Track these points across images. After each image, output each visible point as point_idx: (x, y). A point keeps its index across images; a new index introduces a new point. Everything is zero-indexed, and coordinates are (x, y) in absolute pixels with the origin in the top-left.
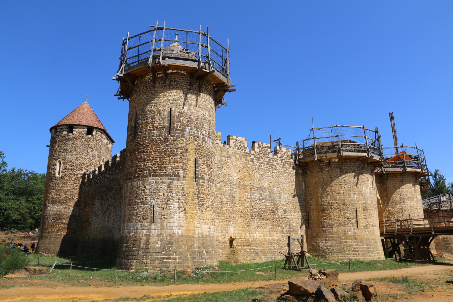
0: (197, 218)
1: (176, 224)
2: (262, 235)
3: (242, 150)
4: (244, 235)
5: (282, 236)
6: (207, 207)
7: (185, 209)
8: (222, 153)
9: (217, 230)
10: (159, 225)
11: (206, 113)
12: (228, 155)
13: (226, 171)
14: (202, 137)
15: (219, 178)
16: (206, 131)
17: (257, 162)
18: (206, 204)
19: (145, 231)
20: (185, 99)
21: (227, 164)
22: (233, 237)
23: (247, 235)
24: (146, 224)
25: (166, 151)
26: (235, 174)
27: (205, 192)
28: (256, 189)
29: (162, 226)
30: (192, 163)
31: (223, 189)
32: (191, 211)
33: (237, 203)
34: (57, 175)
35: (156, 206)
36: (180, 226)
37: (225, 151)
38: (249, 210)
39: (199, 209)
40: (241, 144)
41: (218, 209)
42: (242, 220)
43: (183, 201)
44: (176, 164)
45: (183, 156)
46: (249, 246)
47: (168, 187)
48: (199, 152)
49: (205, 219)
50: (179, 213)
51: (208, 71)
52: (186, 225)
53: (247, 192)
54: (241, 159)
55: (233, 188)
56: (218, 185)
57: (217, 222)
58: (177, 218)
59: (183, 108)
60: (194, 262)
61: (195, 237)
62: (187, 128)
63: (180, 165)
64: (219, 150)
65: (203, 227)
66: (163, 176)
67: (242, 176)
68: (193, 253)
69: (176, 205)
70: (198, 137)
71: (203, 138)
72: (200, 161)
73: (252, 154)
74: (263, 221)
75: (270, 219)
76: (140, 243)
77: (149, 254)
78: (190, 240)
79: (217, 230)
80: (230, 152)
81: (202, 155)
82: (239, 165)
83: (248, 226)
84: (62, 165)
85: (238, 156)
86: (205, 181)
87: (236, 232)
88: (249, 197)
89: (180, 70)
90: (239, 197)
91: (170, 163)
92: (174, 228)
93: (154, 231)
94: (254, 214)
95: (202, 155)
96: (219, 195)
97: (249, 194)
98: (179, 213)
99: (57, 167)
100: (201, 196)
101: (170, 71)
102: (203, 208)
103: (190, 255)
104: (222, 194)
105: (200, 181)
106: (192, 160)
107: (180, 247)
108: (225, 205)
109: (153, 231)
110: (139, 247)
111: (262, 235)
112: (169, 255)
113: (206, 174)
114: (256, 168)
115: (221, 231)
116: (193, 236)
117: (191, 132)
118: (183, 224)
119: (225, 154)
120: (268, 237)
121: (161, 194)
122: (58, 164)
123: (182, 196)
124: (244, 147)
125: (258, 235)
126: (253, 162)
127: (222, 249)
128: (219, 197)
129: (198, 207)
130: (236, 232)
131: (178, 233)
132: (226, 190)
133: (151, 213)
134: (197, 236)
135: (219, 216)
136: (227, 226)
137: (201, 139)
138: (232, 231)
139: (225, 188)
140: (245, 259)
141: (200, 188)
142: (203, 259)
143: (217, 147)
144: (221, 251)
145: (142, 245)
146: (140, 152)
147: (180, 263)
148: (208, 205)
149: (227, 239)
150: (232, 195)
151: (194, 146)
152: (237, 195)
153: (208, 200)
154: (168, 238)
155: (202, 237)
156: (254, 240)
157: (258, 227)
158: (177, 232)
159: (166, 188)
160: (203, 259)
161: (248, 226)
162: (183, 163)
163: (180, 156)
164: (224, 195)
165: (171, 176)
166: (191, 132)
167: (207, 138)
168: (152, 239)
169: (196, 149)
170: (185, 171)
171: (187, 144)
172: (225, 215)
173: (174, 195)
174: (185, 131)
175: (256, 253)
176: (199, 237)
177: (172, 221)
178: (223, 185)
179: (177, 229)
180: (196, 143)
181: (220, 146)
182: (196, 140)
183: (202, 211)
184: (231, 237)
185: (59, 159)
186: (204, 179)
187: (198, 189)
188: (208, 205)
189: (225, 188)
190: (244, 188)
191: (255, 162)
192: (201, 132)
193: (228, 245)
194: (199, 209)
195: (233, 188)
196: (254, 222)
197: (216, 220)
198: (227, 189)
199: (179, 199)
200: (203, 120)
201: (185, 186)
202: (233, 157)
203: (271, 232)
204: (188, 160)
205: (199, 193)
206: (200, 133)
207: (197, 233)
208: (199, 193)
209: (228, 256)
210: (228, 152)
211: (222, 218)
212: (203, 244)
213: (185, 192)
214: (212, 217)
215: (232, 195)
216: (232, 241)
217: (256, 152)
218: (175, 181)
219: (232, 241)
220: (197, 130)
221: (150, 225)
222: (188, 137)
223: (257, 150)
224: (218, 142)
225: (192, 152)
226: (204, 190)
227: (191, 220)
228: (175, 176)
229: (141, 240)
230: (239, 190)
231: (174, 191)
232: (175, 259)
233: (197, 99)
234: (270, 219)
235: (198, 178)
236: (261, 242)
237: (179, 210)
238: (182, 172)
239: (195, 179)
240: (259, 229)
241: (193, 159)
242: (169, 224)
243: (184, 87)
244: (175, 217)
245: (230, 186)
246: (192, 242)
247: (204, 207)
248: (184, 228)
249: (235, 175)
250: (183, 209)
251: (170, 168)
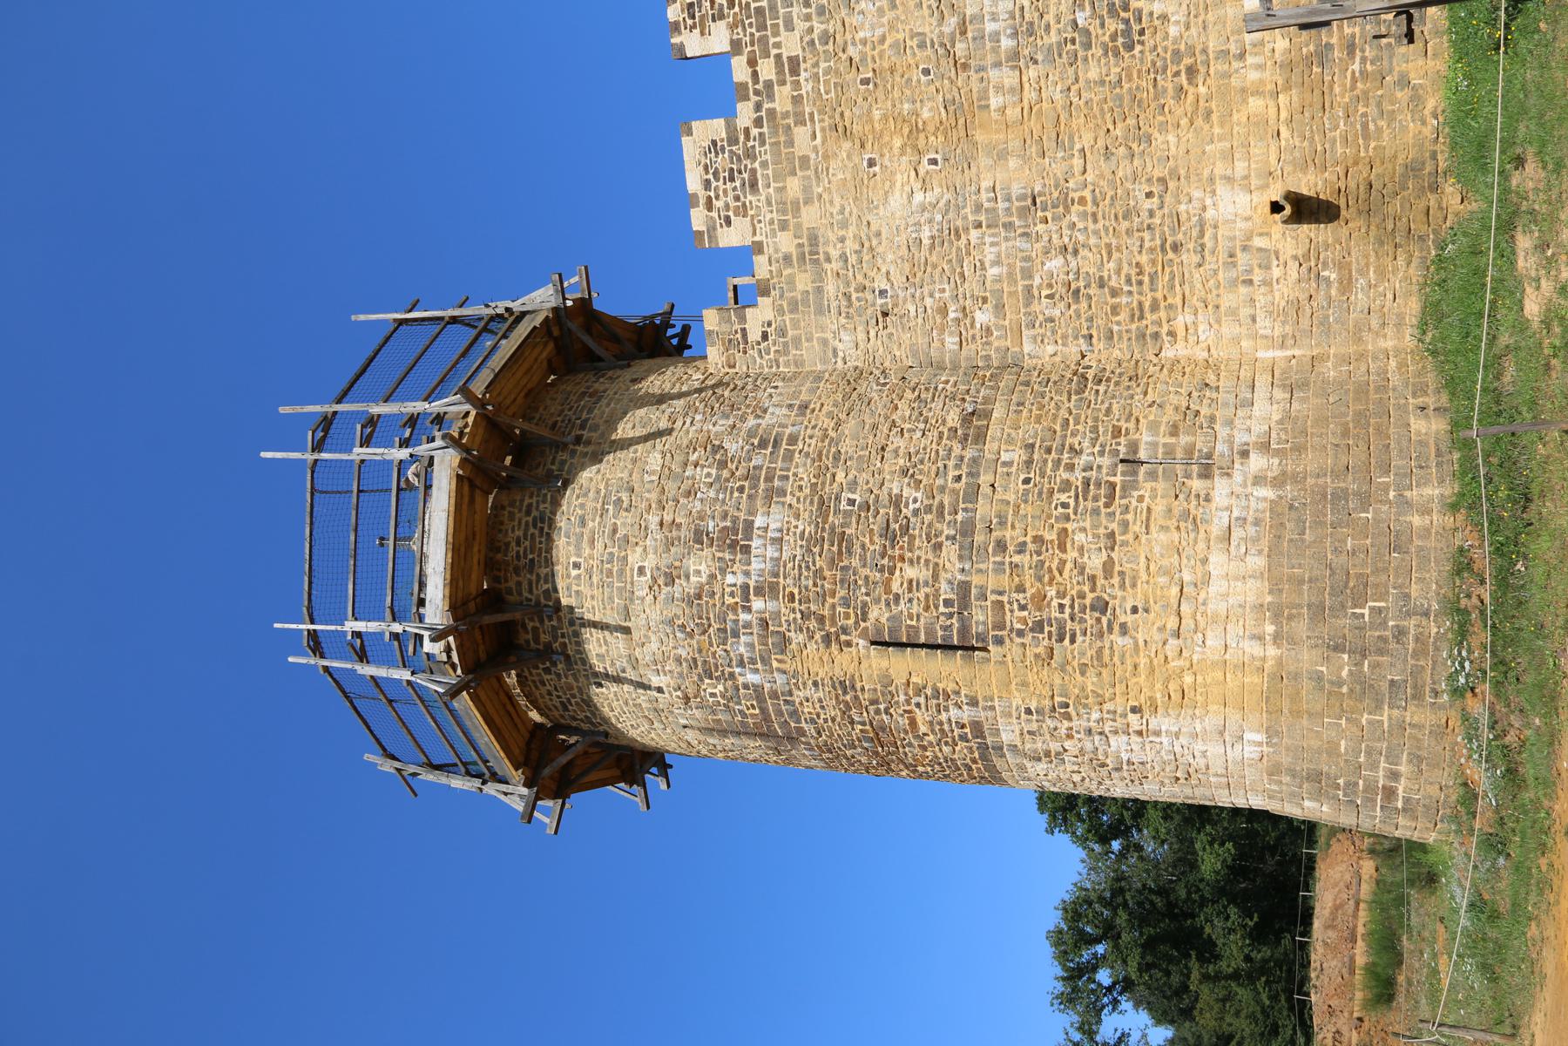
1: (1215, 750)
3: (750, 154)
4: (1255, 104)
6: (1108, 567)
7: (1134, 710)
8: (806, 302)
11: (641, 570)
12: (802, 257)
13: (889, 269)
14: (757, 604)
15: (944, 311)
16: (723, 571)
17: (790, 26)
18: (1093, 579)
20: (618, 680)
21: (853, 259)
23: (1253, 76)
26: (897, 200)
27: (1028, 578)
28: (952, 22)
30: (900, 664)
31: (998, 280)
33: (1058, 169)
36: (1221, 733)
37: (791, 281)
38: (1093, 74)
39: (1124, 629)
40: (722, 161)
41: (1115, 310)
42: (1163, 128)
43: (1095, 716)
44: (923, 729)
45: (874, 702)
48: (833, 623)
49: (1175, 590)
50: (1158, 733)
51: (451, 639)
52: (1213, 708)
53: (984, 95)
54: (805, 160)
55: (978, 208)
56: (982, 317)
57: (1189, 319)
58: (1183, 740)
59: (660, 690)
60: (1418, 696)
61: (1280, 662)
62: (741, 680)
63: (921, 717)
64: (796, 325)
65: (1222, 608)
67: (897, 142)
68: (1364, 689)
71: (759, 591)
72: (878, 614)
73: (755, 75)
78: (1295, 698)
79: (1233, 312)
80: (786, 242)
81: (846, 602)
82: (839, 171)
83: (1192, 72)
85: (794, 186)
86: (976, 580)
87: (1240, 167)
88: (1008, 77)
89: (510, 698)
90: (1025, 159)
92: (1234, 754)
94: (1113, 25)
95: (846, 602)
96: (1035, 307)
97: (993, 74)
98: (1158, 733)
100: (1055, 614)
101: (534, 715)
102: (1122, 600)
103: (1378, 708)
104: (1029, 289)
105: (980, 617)
106: (885, 664)
107: (1332, 750)
108: (1088, 262)
112: (1370, 788)
113: (935, 577)
114: (826, 37)
115: (1243, 290)
116: (1272, 677)
117: (753, 661)
118: (1212, 721)
119: (804, 282)
123: (1068, 717)
124: (733, 140)
126: (795, 64)
127: (1346, 285)
128: (1042, 307)
129: (1120, 641)
130: (1240, 167)
131: (1260, 744)
132: (997, 263)
134: (1272, 651)
135: (1155, 307)
136: (1207, 239)
137: (772, 605)
138: (1237, 207)
139: (993, 271)
140: (1416, 100)
141: (1014, 618)
142: (1400, 633)
143: (782, 332)
144: (1360, 298)
147: (1416, 759)
148: (1095, 563)
150: (1024, 213)
151: (812, 647)
152: (1016, 176)
153: (1072, 554)
155: (1277, 617)
160: (1400, 633)
161: (1192, 72)
162: (908, 702)
163: (878, 712)
164: (1028, 274)
166: (753, 661)
167: (756, 565)
169: (827, 640)
171: (815, 684)
172: (1144, 259)
174: (758, 689)
176: (1277, 638)
177: (1201, 762)
178: (972, 286)
179: (1238, 747)
180: (797, 638)
181: (769, 314)
182: (784, 641)
183: (1135, 610)
184: (1276, 208)
187: (1020, 633)
188: (1095, 563)
189: (993, 271)
190: (962, 116)
191: (791, 44)
192: (734, 608)
194: (1124, 629)
195: (978, 208)
196: (1164, 18)
198: (993, 252)
200: (677, 590)
202: (810, 216)
205: (1039, 627)
206: (744, 617)
207: (1254, 649)
208: (1039, 627)
209: (1393, 238)
210: (787, 258)
212: (1318, 611)
213: (1047, 703)
215: (1024, 213)
217: (736, 47)
220: (736, 635)
222: (780, 679)
223: (718, 39)
224: (754, 335)
225: (843, 663)
226: (1021, 589)
227: (1188, 679)
230: (984, 161)
232: (1395, 776)
233: (595, 625)
235: (964, 630)
237: (1140, 733)
239: (974, 649)
241: (879, 662)
243: (571, 680)
244: (1177, 749)
245: (974, 234)
246: (1307, 685)
247: (1111, 590)
248: (1234, 717)
249: (903, 202)
250: (1133, 719)
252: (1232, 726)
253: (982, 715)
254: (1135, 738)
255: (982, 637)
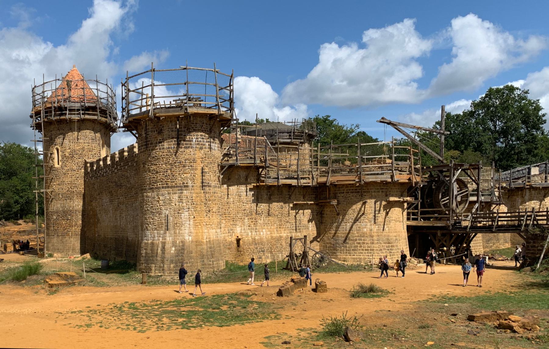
0: (205, 224)
1: (187, 231)
2: (269, 233)
4: (250, 234)
5: (291, 232)
6: (213, 212)
9: (225, 230)
10: (173, 233)
19: (161, 239)
22: (240, 237)
24: (162, 232)
25: (175, 163)
29: (175, 233)
30: (199, 172)
32: (199, 218)
34: (56, 165)
35: (169, 215)
39: (207, 215)
44: (185, 175)
45: (191, 166)
46: (256, 244)
47: (179, 197)
63: (189, 175)
66: (174, 187)
69: (187, 213)
70: (204, 145)
72: (206, 170)
74: (270, 218)
75: (277, 216)
76: (157, 250)
77: (165, 260)
79: (225, 230)
84: (60, 153)
87: (243, 231)
91: (179, 174)
92: (186, 235)
93: (169, 239)
99: (55, 156)
105: (207, 189)
108: (232, 205)
109: (168, 239)
110: (157, 253)
111: (269, 233)
118: (192, 231)
120: (275, 235)
121: (173, 204)
122: (55, 151)
123: (192, 205)
125: (265, 233)
129: (205, 214)
130: (243, 231)
133: (165, 222)
138: (238, 231)
145: (159, 251)
146: (152, 164)
148: (214, 210)
149: (234, 239)
150: (239, 195)
154: (181, 244)
156: (261, 239)
157: (265, 224)
158: (188, 238)
159: (177, 198)
165: (180, 187)
168: (167, 246)
169: (202, 158)
170: (193, 180)
173: (185, 204)
175: (262, 251)
180: (202, 152)
185: (56, 147)
186: (210, 186)
188: (214, 210)
193: (236, 245)
194: (207, 215)
197: (223, 221)
199: (189, 208)
201: (194, 195)
203: (279, 229)
204: (196, 169)
211: (229, 218)
214: (219, 221)
215: (239, 195)
216: (238, 241)
218: (185, 192)
219: (238, 241)
220: (202, 138)
221: (165, 233)
222: (194, 146)
225: (199, 161)
227: (200, 226)
228: (185, 186)
229: (158, 246)
231: (184, 201)
234: (277, 216)
235: (205, 186)
236: (267, 241)
238: (190, 182)
240: (266, 227)
241: (199, 168)
242: (181, 232)
247: (211, 213)
248: (194, 235)
250: (193, 217)
251: (180, 179)
252: (192, 234)
253: (191, 188)
254: (188, 217)
255: (204, 189)
